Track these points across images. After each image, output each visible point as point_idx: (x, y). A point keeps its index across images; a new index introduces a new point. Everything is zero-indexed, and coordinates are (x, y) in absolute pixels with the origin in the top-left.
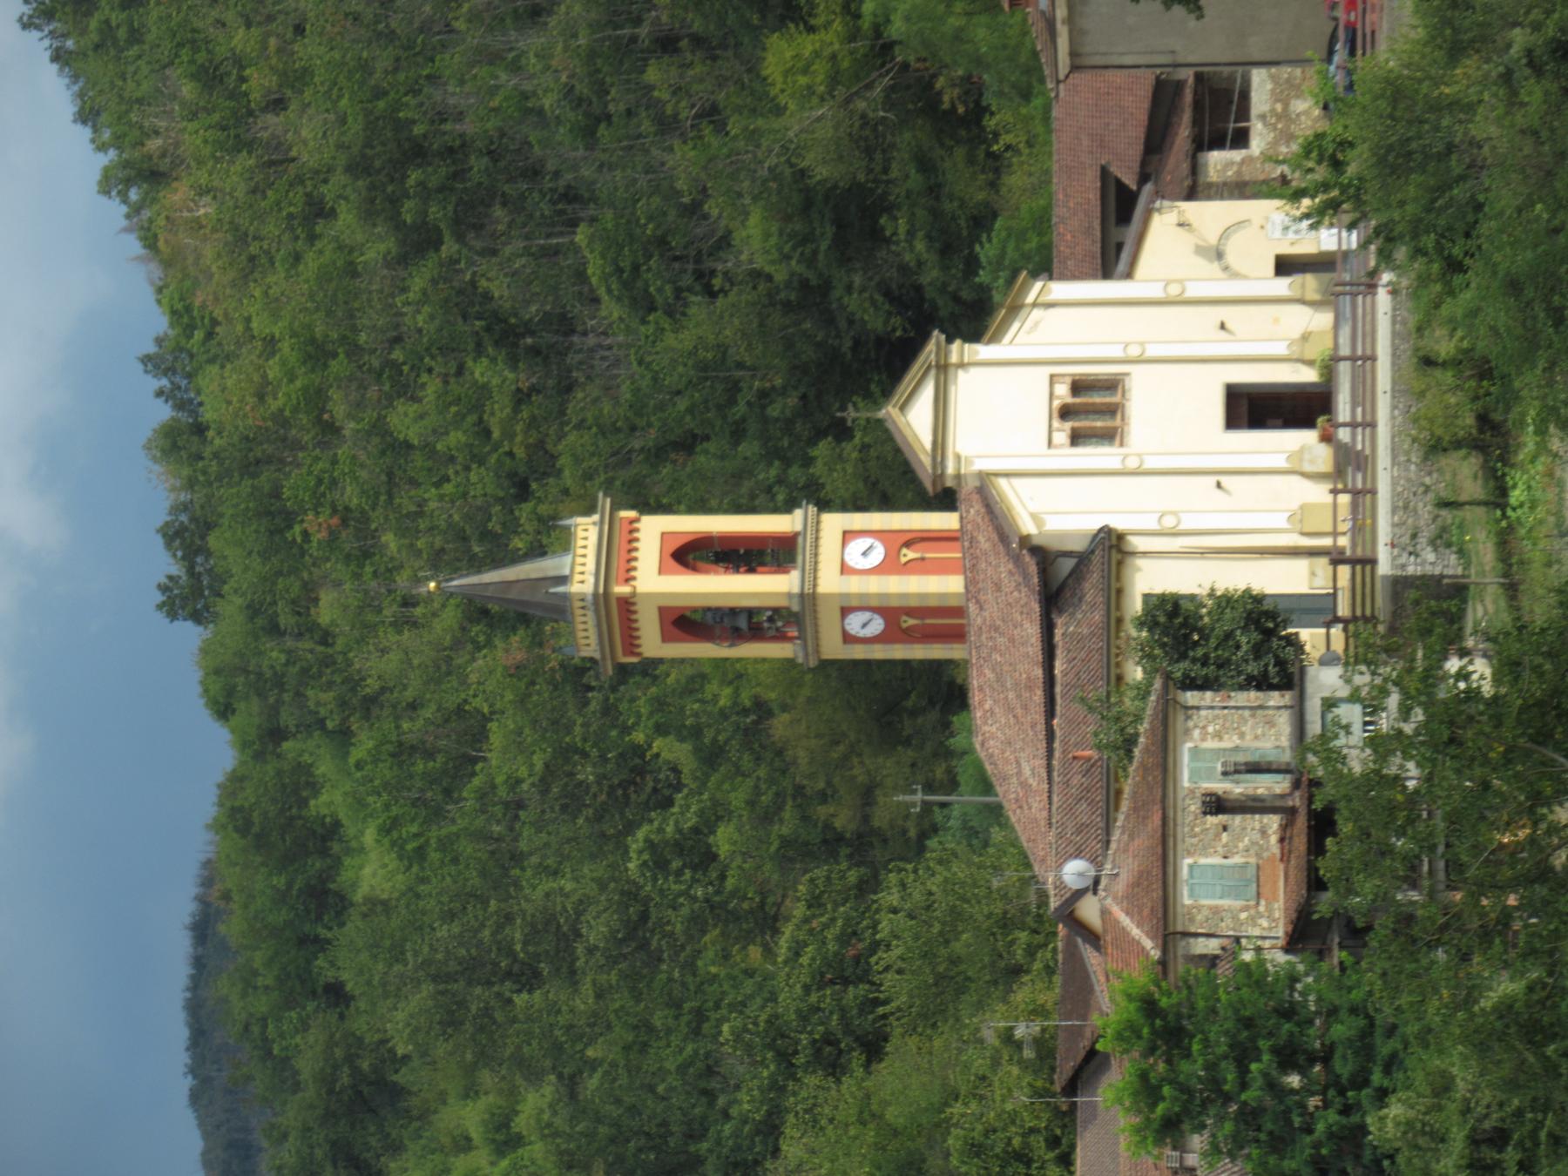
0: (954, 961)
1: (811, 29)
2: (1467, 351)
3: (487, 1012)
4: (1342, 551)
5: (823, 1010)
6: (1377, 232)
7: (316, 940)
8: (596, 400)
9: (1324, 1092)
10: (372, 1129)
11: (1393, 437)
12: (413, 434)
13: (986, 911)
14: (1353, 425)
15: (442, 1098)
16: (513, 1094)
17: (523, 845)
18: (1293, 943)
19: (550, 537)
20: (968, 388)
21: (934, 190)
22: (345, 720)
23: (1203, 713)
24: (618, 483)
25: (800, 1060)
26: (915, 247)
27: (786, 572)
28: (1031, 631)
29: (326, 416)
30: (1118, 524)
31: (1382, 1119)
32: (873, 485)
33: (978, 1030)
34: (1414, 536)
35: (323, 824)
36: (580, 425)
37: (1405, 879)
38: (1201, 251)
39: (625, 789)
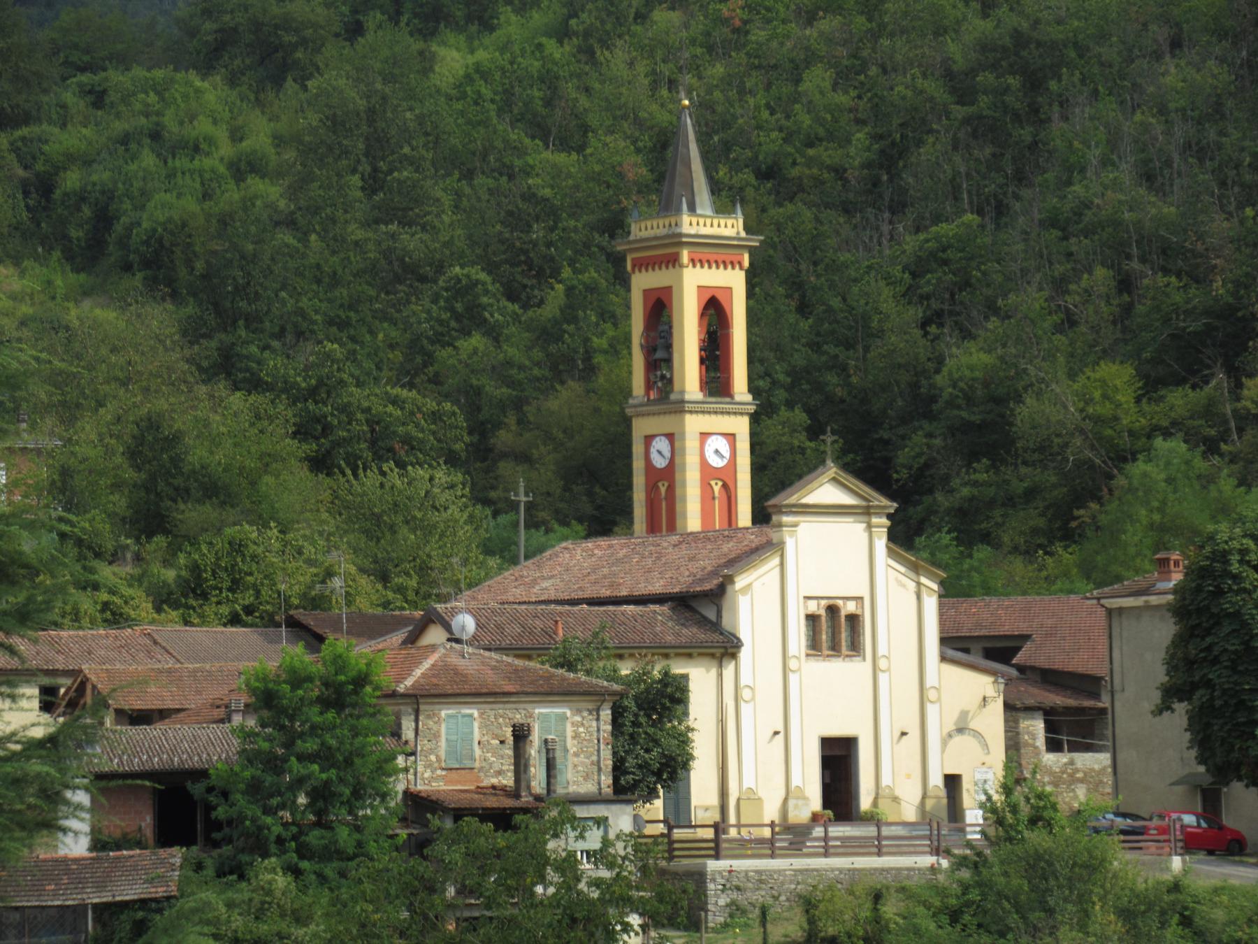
0: (392, 529)
1: (1138, 400)
2: (887, 926)
3: (346, 152)
4: (725, 832)
5: (349, 423)
6: (979, 854)
7: (399, 13)
8: (838, 233)
9: (293, 823)
10: (248, 61)
11: (817, 870)
12: (805, 86)
13: (434, 553)
14: (826, 838)
15: (274, 118)
16: (279, 174)
17: (480, 180)
18: (412, 798)
19: (725, 197)
20: (852, 533)
21: (1010, 502)
22: (576, 34)
23: (594, 724)
24: (771, 252)
25: (311, 406)
26: (959, 490)
27: (701, 390)
28: (657, 587)
29: (821, 13)
30: (744, 654)
31: (274, 871)
32: (773, 456)
33: (337, 548)
34: (738, 888)
35: (492, 18)
36: (817, 219)
37: (464, 886)
38: (964, 715)
39: (525, 262)
